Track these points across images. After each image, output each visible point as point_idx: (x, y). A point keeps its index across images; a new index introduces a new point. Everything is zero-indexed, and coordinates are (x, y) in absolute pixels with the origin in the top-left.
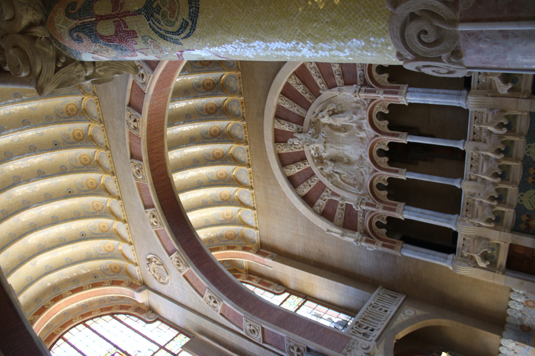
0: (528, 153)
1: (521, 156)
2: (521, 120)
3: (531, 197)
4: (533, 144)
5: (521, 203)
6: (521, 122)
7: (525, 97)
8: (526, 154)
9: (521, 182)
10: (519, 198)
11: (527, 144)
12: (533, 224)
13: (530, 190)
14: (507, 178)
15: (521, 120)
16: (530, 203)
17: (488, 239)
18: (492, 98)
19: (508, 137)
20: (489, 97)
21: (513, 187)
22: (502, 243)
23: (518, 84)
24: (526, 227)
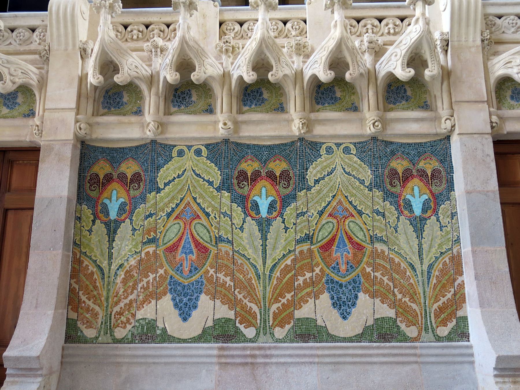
0: (329, 150)
1: (319, 131)
2: (422, 120)
3: (198, 175)
4: (356, 159)
5: (174, 154)
6: (417, 120)
7: (494, 119)
8: (324, 146)
9: (237, 144)
10: (189, 147)
11: (355, 144)
12: (115, 192)
13: (220, 169)
14: (246, 108)
15: (422, 120)
16: (179, 177)
17: (43, 82)
18: (479, 42)
19: (371, 93)
20: (482, 35)
21: (225, 124)
22: (37, 121)
23: (513, 102)
24: (101, 177)
